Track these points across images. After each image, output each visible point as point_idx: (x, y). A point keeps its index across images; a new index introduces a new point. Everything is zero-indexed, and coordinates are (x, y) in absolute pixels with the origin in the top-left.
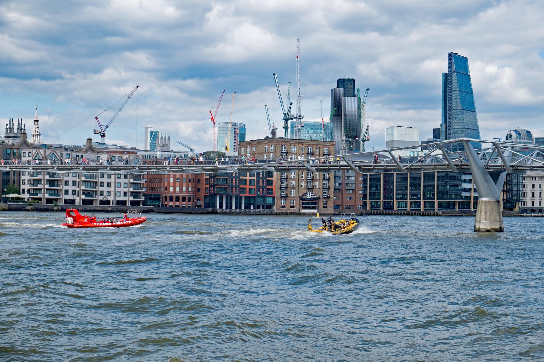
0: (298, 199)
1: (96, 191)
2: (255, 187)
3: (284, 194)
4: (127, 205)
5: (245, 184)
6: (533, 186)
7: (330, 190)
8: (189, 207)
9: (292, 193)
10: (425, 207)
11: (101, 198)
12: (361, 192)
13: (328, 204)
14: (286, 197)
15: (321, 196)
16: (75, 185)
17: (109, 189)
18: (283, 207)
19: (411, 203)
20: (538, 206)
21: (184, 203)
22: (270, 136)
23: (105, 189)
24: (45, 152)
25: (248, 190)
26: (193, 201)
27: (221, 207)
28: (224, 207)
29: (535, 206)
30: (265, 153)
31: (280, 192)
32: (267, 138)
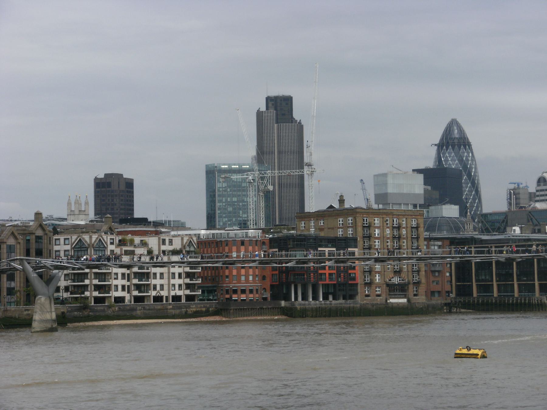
0: (385, 285)
3: (368, 280)
7: (421, 273)
9: (377, 277)
10: (520, 291)
11: (154, 293)
12: (448, 274)
13: (419, 291)
14: (369, 284)
16: (125, 279)
17: (162, 282)
18: (367, 296)
21: (251, 295)
22: (336, 205)
24: (91, 237)
27: (296, 299)
28: (300, 298)
30: (339, 228)
31: (363, 277)
32: (331, 207)
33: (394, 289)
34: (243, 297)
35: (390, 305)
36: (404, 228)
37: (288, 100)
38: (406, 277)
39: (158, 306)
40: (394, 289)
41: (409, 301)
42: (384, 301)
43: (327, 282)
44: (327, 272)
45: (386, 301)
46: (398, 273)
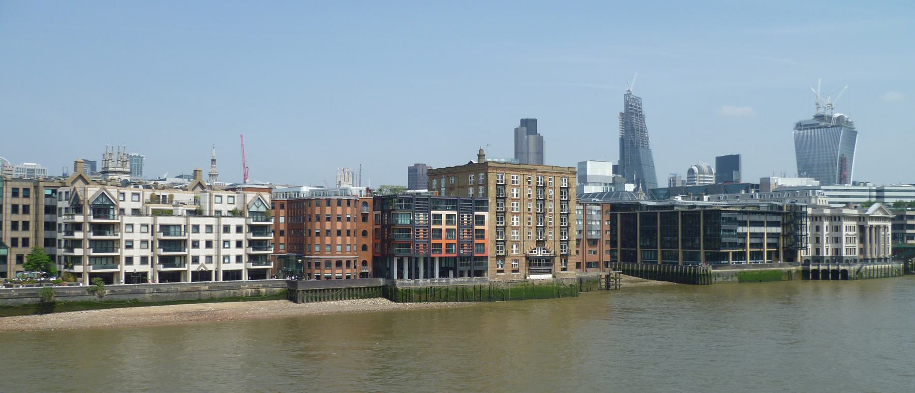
1: (185, 256)
2: (455, 241)
4: (243, 279)
5: (440, 237)
6: (818, 229)
7: (570, 243)
8: (348, 277)
11: (194, 267)
15: (558, 253)
23: (202, 252)
25: (444, 246)
26: (355, 267)
33: (534, 264)
34: (338, 273)
35: (530, 282)
37: (534, 121)
39: (203, 286)
40: (534, 264)
41: (554, 277)
43: (444, 254)
44: (443, 241)
46: (541, 243)
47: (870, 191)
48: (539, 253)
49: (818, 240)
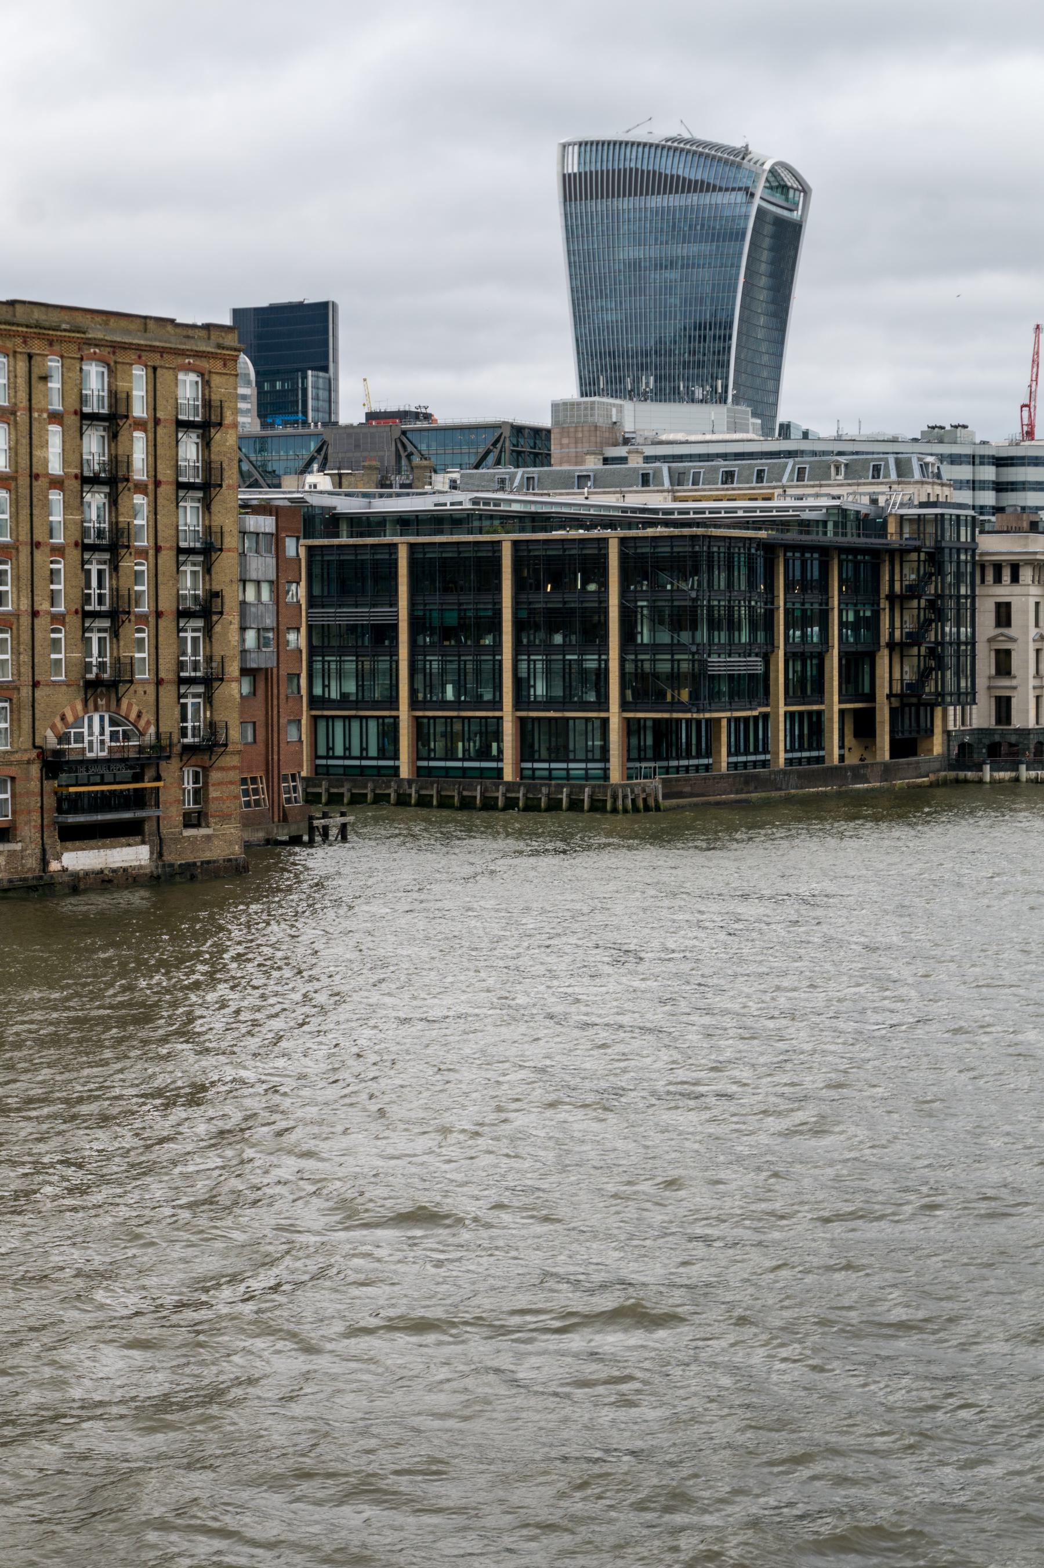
0: (35, 770)
6: (1004, 614)
10: (526, 751)
13: (213, 793)
19: (420, 728)
20: (1032, 724)
29: (1017, 723)
36: (140, 424)
38: (148, 716)
42: (32, 862)
45: (44, 862)
46: (102, 688)
47: (973, 460)
48: (95, 736)
49: (1003, 663)
